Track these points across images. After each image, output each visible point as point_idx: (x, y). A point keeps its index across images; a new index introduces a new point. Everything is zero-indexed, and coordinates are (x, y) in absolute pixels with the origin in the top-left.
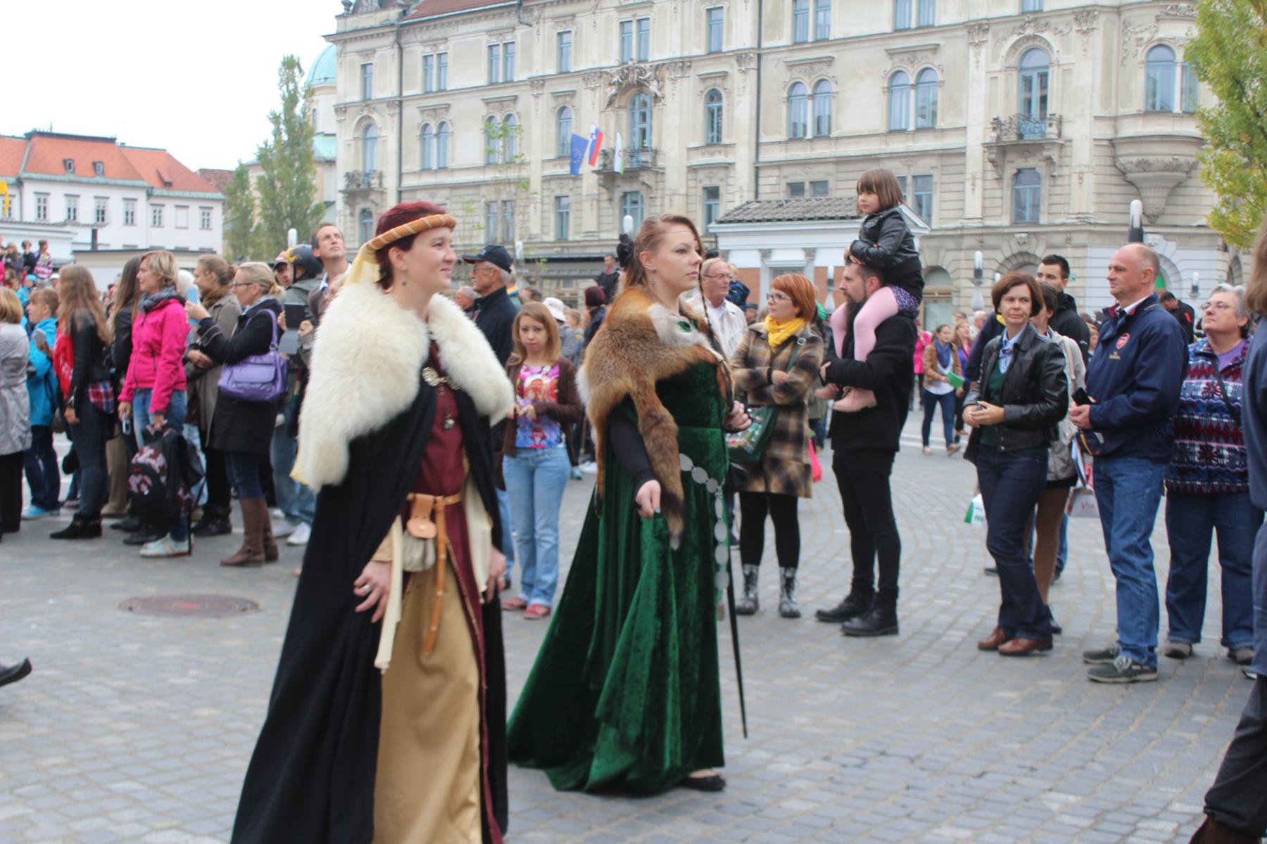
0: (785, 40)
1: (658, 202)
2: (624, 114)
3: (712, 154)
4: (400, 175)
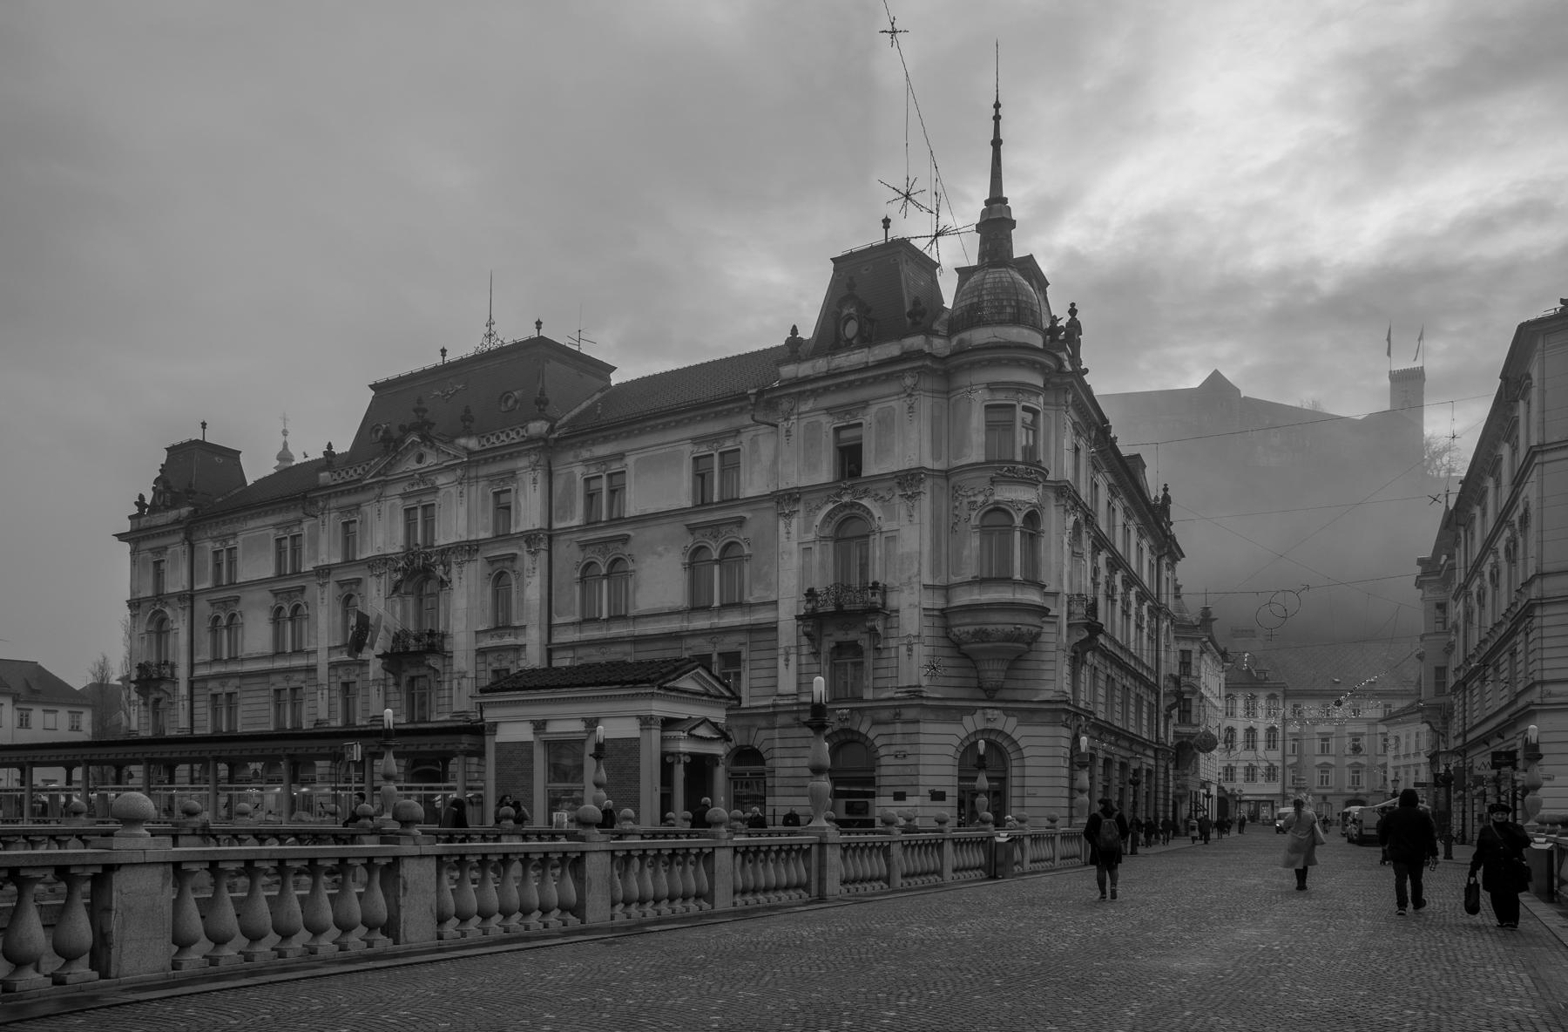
0: (577, 520)
1: (446, 685)
2: (411, 601)
3: (501, 637)
4: (192, 666)
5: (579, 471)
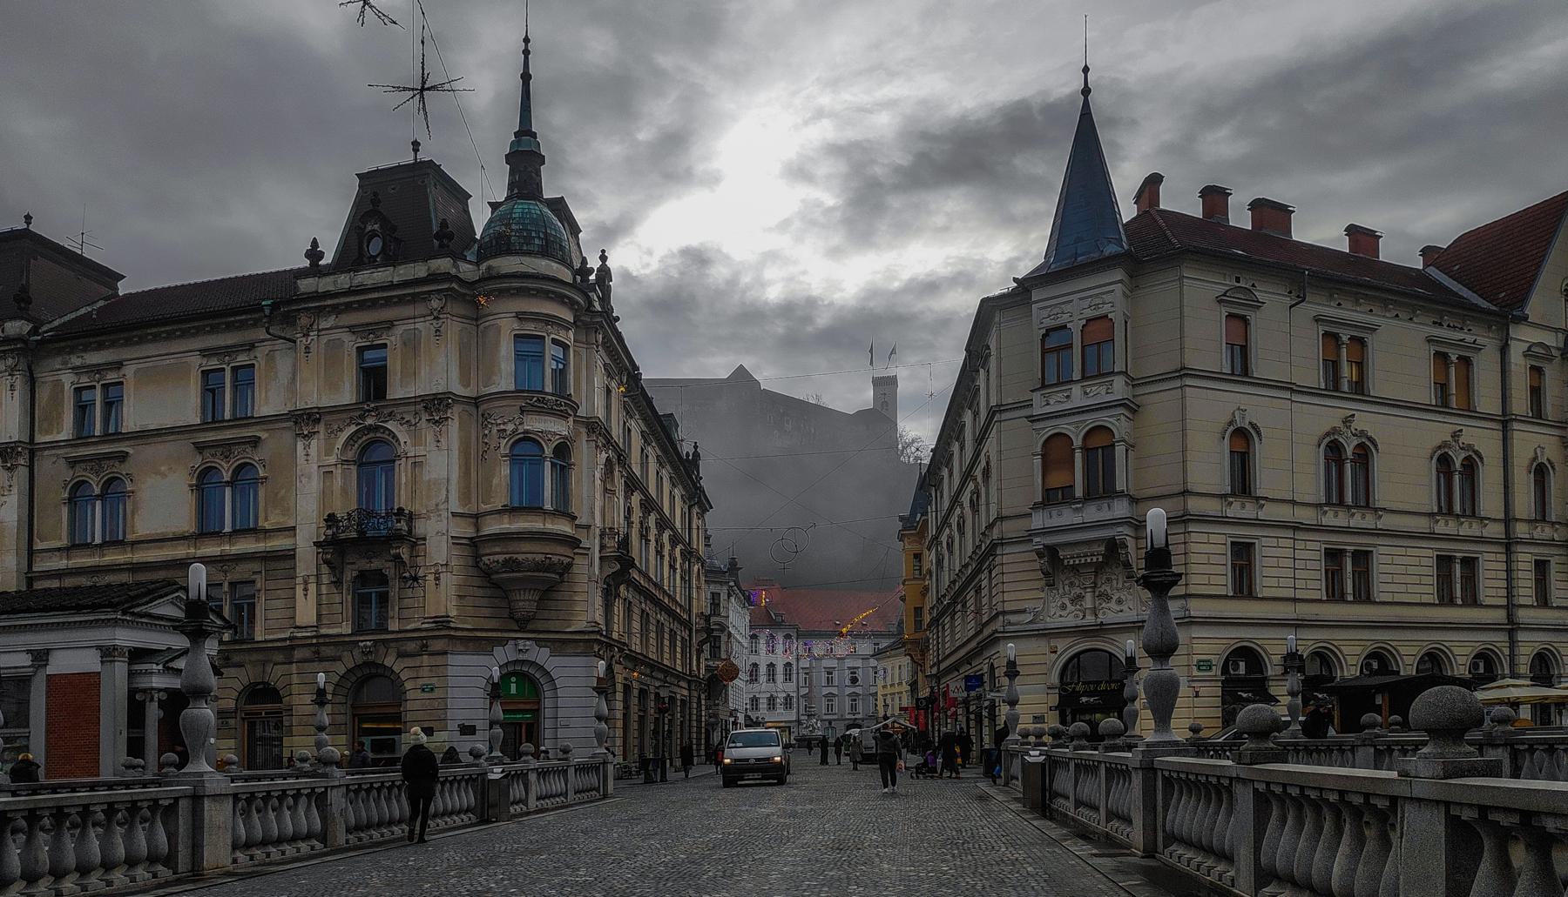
5: (68, 380)
